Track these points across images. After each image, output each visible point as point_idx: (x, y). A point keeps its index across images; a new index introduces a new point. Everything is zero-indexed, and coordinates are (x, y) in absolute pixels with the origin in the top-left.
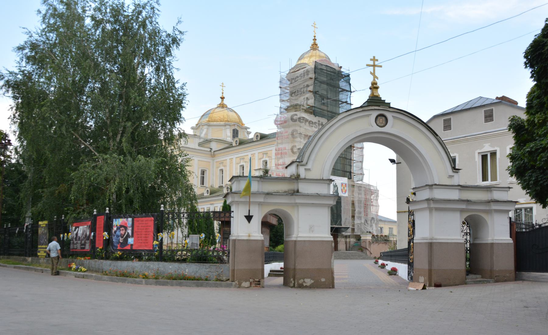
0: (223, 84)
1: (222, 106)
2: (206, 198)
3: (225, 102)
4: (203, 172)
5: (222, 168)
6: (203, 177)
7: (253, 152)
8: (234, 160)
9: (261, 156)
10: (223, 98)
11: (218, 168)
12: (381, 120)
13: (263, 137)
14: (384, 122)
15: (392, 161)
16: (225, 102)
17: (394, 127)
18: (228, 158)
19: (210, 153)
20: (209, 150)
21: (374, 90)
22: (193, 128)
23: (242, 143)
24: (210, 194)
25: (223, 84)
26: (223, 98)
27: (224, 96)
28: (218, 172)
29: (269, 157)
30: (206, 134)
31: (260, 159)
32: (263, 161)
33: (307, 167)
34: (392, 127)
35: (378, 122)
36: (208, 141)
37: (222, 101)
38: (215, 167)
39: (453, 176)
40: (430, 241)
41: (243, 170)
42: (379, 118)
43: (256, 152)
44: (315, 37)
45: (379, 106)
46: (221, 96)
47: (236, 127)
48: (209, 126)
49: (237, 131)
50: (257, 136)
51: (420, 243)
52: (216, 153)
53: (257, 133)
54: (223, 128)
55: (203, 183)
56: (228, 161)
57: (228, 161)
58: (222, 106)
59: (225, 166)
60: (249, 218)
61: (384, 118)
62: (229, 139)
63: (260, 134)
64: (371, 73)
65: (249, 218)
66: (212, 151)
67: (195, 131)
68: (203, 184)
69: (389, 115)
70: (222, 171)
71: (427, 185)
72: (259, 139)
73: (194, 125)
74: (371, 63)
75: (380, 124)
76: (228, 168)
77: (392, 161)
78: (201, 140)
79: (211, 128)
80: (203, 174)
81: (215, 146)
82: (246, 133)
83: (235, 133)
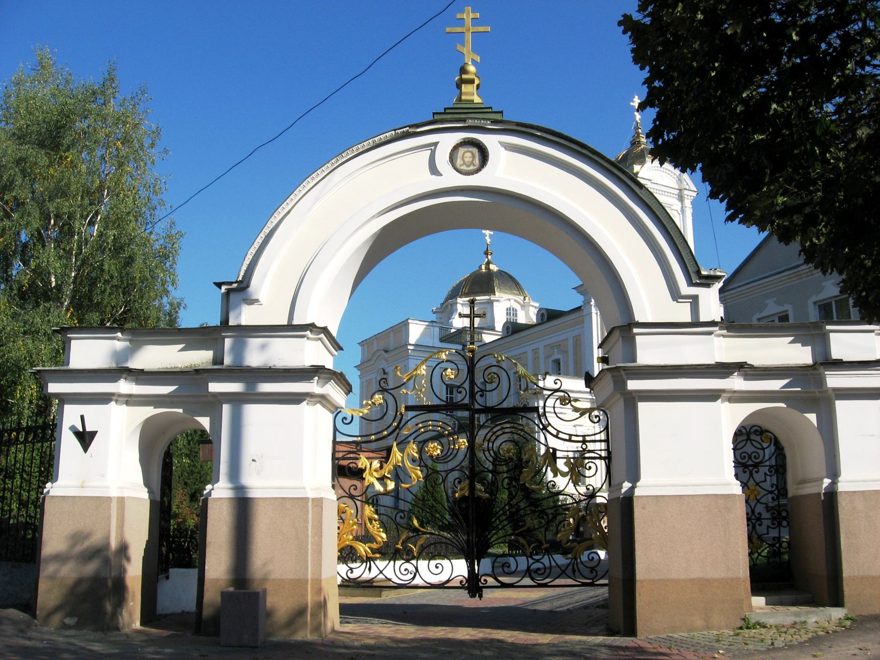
7: (535, 346)
12: (468, 155)
14: (477, 162)
35: (459, 162)
43: (541, 345)
45: (464, 120)
50: (543, 315)
60: (85, 438)
61: (475, 151)
65: (85, 438)
69: (490, 141)
72: (545, 319)
75: (464, 168)
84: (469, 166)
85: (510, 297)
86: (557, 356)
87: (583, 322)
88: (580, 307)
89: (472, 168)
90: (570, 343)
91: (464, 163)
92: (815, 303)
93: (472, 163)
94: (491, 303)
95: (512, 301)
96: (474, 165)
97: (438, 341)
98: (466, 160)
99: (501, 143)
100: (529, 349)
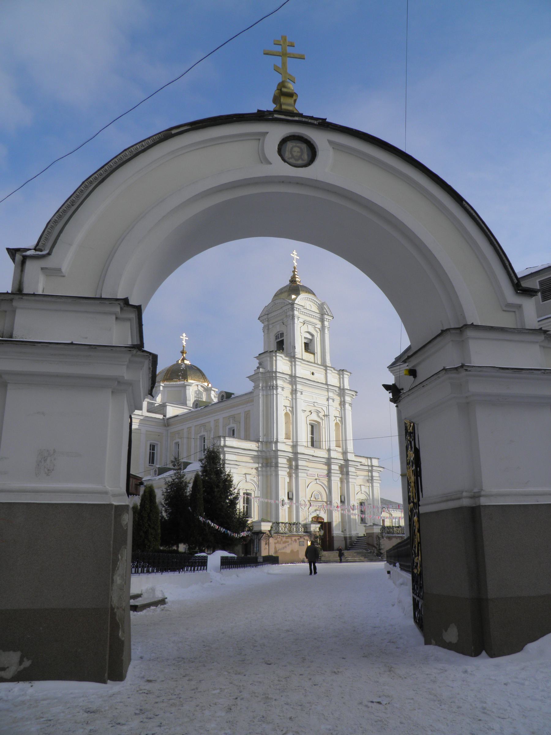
4: (153, 447)
5: (178, 440)
6: (153, 454)
12: (296, 150)
14: (306, 157)
17: (331, 165)
21: (283, 100)
32: (229, 429)
33: (48, 263)
35: (287, 155)
39: (520, 306)
40: (466, 502)
41: (204, 442)
50: (223, 396)
51: (437, 513)
59: (181, 438)
61: (304, 146)
63: (226, 392)
64: (276, 69)
68: (153, 463)
69: (319, 138)
70: (178, 444)
71: (443, 332)
74: (278, 49)
80: (153, 449)
85: (200, 383)
86: (232, 425)
87: (252, 401)
89: (300, 162)
90: (242, 416)
91: (293, 157)
93: (300, 158)
94: (184, 386)
96: (303, 160)
98: (295, 154)
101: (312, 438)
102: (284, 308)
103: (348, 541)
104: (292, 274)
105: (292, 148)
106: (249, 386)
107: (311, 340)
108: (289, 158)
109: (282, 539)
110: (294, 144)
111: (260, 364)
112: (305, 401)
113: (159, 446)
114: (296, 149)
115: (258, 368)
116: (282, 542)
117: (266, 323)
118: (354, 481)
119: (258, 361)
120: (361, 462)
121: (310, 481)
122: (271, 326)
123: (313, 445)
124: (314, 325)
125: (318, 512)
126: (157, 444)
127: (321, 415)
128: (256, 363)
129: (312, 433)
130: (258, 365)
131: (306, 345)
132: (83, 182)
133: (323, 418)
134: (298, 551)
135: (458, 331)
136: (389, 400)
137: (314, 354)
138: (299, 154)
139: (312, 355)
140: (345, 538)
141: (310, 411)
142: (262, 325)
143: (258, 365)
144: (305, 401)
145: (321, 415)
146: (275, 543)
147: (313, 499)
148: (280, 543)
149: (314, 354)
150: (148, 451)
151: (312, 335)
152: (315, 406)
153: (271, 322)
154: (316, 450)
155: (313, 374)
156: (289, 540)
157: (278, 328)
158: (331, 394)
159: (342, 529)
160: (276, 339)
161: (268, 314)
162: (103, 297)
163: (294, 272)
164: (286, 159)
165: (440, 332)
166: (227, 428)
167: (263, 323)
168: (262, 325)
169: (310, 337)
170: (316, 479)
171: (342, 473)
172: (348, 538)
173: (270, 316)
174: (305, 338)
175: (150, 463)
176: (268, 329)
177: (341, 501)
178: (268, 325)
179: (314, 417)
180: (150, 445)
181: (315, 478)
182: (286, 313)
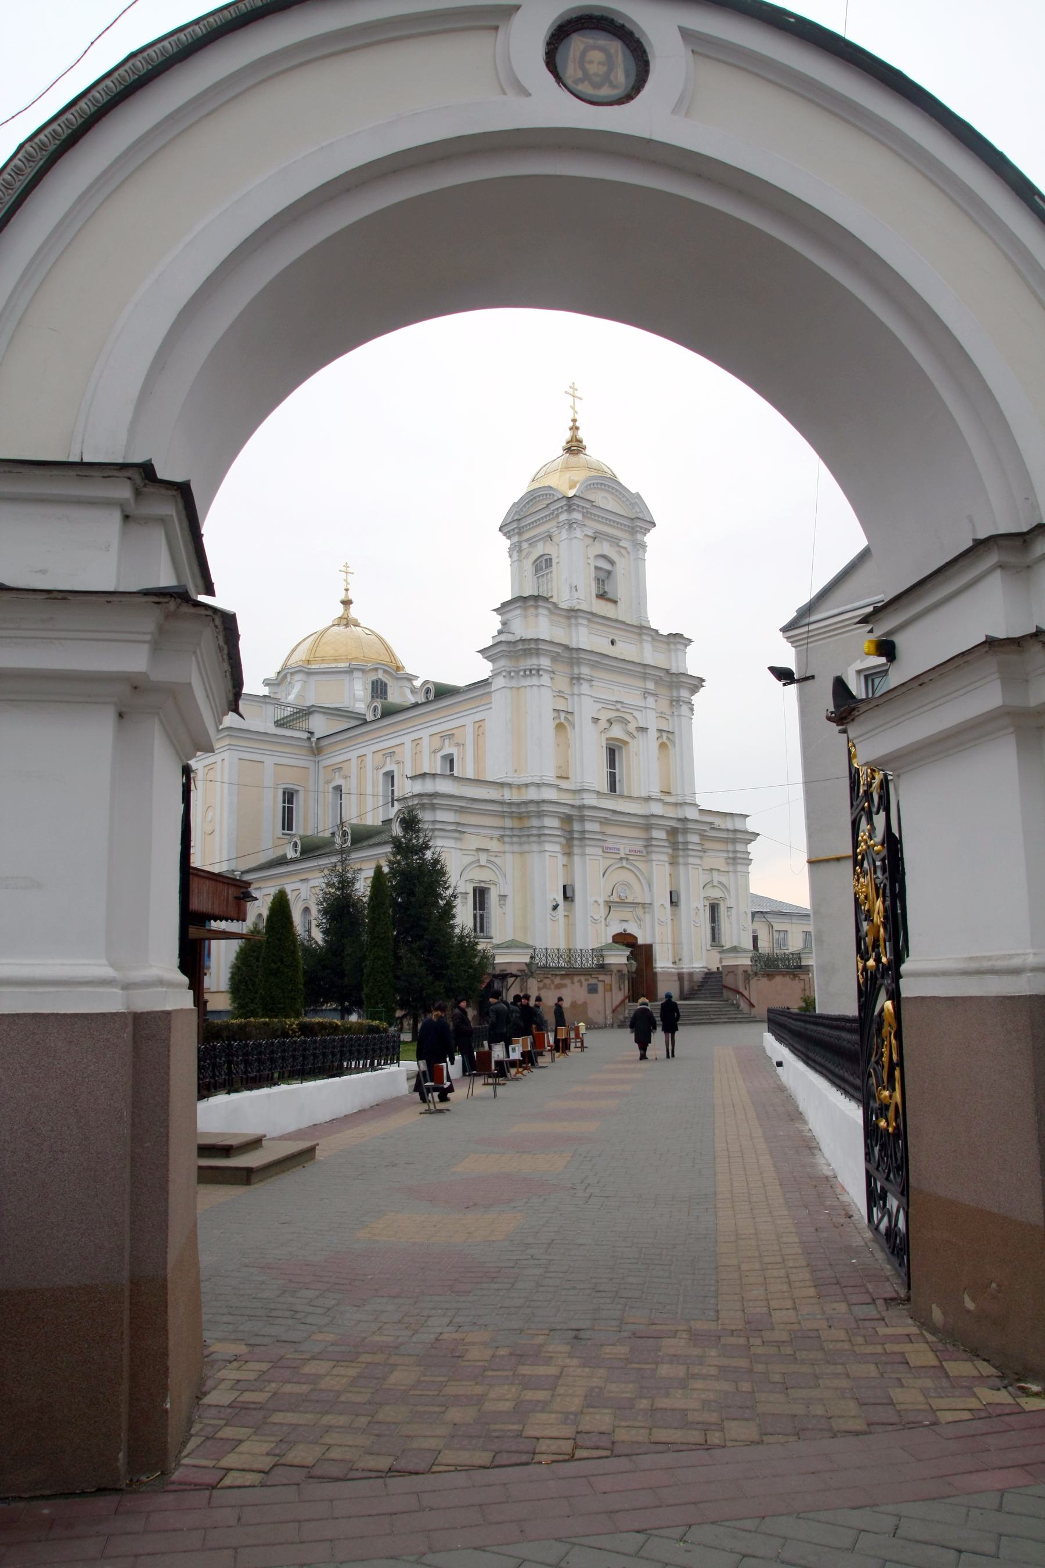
0: (346, 566)
1: (346, 621)
2: (293, 861)
3: (354, 612)
4: (289, 796)
6: (290, 810)
8: (369, 759)
9: (437, 742)
10: (347, 603)
11: (328, 782)
13: (442, 693)
14: (621, 78)
15: (783, 675)
16: (354, 612)
18: (353, 755)
19: (306, 744)
20: (305, 735)
22: (267, 683)
23: (389, 712)
24: (301, 854)
25: (346, 566)
26: (347, 603)
27: (351, 597)
28: (330, 796)
29: (458, 745)
30: (299, 696)
31: (435, 752)
32: (444, 757)
34: (684, 106)
35: (571, 72)
36: (305, 713)
37: (346, 610)
38: (321, 782)
41: (393, 785)
42: (577, 43)
43: (424, 734)
44: (574, 421)
46: (342, 597)
47: (380, 675)
48: (310, 673)
49: (384, 686)
50: (428, 691)
51: (952, 1001)
52: (324, 743)
53: (426, 682)
54: (346, 678)
55: (288, 822)
56: (354, 763)
57: (354, 763)
58: (346, 621)
59: (345, 777)
61: (616, 47)
62: (360, 707)
63: (435, 684)
66: (314, 739)
67: (275, 689)
68: (290, 828)
70: (338, 789)
71: (980, 546)
72: (432, 696)
73: (272, 675)
75: (585, 88)
76: (354, 781)
77: (783, 675)
78: (282, 714)
79: (313, 679)
80: (290, 801)
81: (320, 725)
82: (408, 692)
83: (379, 689)
84: (597, 86)
88: (487, 680)
89: (605, 92)
90: (470, 730)
91: (586, 77)
92: (859, 672)
93: (606, 79)
95: (380, 672)
96: (613, 86)
97: (273, 725)
98: (592, 69)
99: (686, 34)
100: (407, 740)
101: (612, 777)
102: (553, 507)
103: (686, 984)
104: (568, 435)
105: (584, 54)
106: (483, 669)
107: (609, 573)
108: (577, 81)
109: (552, 981)
110: (591, 41)
111: (504, 623)
112: (597, 700)
113: (301, 794)
114: (596, 56)
115: (500, 632)
116: (553, 986)
117: (516, 539)
118: (698, 861)
119: (499, 618)
120: (712, 823)
121: (609, 862)
122: (525, 545)
123: (613, 787)
124: (615, 541)
125: (625, 926)
126: (297, 791)
127: (631, 727)
128: (495, 623)
129: (612, 764)
130: (500, 626)
131: (600, 582)
132: (21, 147)
133: (635, 733)
134: (585, 1003)
135: (1018, 542)
136: (824, 714)
137: (615, 602)
138: (603, 70)
139: (610, 605)
140: (680, 976)
141: (608, 720)
142: (507, 543)
143: (500, 626)
144: (597, 700)
145: (631, 727)
146: (539, 989)
147: (615, 898)
148: (550, 989)
149: (615, 602)
150: (280, 805)
151: (612, 563)
152: (618, 710)
153: (526, 536)
154: (620, 801)
155: (613, 642)
156: (567, 981)
157: (540, 549)
158: (650, 685)
159: (674, 957)
160: (536, 571)
161: (519, 520)
162: (85, 460)
163: (575, 428)
164: (569, 82)
165: (970, 544)
166: (440, 755)
167: (509, 538)
168: (507, 543)
169: (606, 566)
170: (621, 859)
171: (674, 845)
172: (686, 978)
173: (523, 523)
174: (596, 568)
175: (284, 829)
176: (520, 551)
177: (672, 902)
178: (520, 542)
179: (617, 732)
180: (284, 793)
181: (618, 857)
182: (557, 516)
